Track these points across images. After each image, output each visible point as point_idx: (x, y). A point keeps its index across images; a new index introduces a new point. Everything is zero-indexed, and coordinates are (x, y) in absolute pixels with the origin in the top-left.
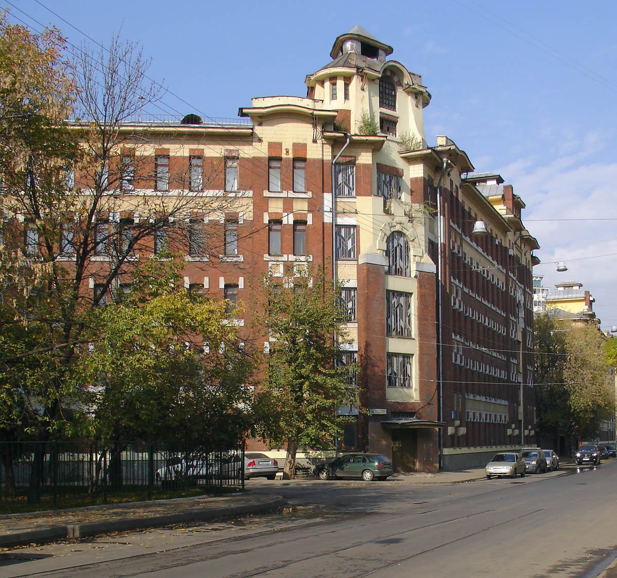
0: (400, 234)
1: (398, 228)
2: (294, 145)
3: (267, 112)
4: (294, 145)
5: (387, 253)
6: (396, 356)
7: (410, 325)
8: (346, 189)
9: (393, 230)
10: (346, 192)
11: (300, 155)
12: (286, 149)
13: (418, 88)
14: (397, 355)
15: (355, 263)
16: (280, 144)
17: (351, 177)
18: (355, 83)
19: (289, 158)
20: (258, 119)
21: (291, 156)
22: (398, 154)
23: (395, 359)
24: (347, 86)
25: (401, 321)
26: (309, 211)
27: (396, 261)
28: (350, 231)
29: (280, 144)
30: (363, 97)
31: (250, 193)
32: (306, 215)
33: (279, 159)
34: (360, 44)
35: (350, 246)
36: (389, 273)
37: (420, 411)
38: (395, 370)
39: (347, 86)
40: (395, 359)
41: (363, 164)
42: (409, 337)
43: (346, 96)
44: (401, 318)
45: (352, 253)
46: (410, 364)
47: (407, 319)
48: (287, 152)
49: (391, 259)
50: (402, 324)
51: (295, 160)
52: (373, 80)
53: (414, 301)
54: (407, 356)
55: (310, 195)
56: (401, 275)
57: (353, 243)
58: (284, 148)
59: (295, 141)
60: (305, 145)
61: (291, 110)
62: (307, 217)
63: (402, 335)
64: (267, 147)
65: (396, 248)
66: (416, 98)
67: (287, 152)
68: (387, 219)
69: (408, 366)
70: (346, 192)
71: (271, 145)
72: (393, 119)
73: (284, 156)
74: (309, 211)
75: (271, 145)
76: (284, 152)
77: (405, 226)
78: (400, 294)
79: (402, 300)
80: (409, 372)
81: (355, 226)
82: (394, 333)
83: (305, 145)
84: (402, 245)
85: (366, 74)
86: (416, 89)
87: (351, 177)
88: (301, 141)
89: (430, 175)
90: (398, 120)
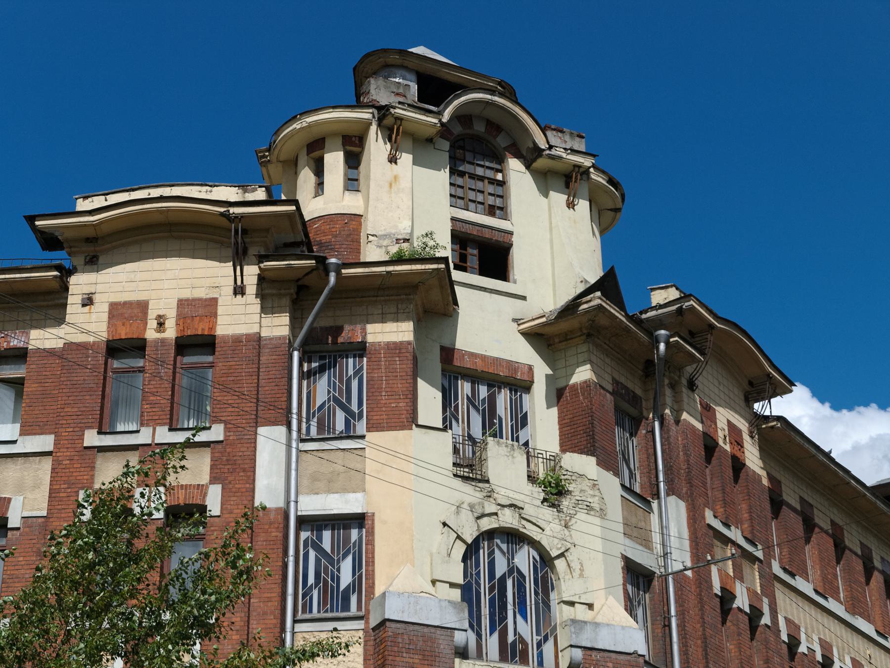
0: (515, 537)
1: (508, 519)
2: (182, 303)
3: (102, 222)
4: (182, 303)
5: (469, 592)
8: (340, 417)
9: (487, 524)
10: (340, 426)
11: (200, 328)
12: (159, 317)
13: (564, 155)
15: (360, 624)
16: (143, 307)
17: (355, 384)
19: (163, 341)
20: (90, 249)
21: (171, 333)
22: (515, 325)
24: (353, 160)
26: (213, 480)
27: (504, 618)
28: (347, 539)
29: (143, 307)
30: (396, 178)
31: (45, 442)
32: (202, 489)
33: (138, 347)
34: (414, 77)
35: (346, 578)
39: (353, 160)
41: (388, 344)
43: (352, 183)
45: (354, 599)
48: (161, 325)
49: (485, 611)
51: (184, 345)
52: (430, 140)
55: (217, 433)
57: (356, 567)
58: (152, 314)
59: (187, 294)
60: (212, 304)
61: (168, 210)
62: (205, 495)
64: (105, 317)
65: (503, 580)
66: (567, 186)
67: (161, 325)
68: (469, 493)
70: (340, 426)
71: (117, 311)
72: (497, 237)
73: (151, 334)
74: (213, 480)
75: (117, 311)
76: (152, 324)
77: (530, 511)
81: (359, 520)
83: (212, 304)
84: (525, 571)
85: (399, 119)
86: (561, 158)
87: (355, 384)
88: (201, 293)
89: (623, 380)
90: (515, 239)
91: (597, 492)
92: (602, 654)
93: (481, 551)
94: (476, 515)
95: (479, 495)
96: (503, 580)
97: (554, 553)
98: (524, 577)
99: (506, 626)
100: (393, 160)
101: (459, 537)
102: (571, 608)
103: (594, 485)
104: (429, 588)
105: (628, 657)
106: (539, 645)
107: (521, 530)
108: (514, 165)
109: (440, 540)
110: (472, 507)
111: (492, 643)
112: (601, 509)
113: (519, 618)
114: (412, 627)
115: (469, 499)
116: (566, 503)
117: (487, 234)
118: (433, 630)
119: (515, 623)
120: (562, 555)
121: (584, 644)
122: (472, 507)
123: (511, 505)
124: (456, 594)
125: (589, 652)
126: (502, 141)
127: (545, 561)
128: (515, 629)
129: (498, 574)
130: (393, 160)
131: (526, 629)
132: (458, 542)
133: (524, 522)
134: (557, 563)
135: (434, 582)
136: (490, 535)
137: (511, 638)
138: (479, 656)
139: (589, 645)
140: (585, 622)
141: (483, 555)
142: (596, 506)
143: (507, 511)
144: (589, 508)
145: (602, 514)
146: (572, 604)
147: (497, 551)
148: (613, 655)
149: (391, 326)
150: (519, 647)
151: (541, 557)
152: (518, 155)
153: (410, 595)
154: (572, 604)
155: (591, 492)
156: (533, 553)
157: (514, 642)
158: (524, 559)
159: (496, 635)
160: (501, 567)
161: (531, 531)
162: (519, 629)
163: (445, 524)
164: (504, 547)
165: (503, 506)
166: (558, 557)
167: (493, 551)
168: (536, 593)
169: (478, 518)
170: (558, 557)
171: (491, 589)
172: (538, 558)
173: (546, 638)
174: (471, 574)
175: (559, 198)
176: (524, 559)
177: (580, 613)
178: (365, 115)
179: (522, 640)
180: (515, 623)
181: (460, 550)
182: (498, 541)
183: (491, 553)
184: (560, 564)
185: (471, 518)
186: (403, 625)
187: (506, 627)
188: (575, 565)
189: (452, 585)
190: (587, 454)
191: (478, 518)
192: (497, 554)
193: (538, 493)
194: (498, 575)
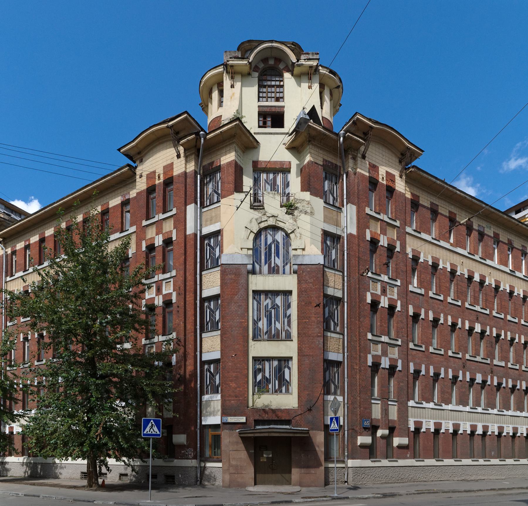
0: (275, 228)
1: (271, 222)
5: (256, 250)
6: (267, 360)
7: (290, 327)
9: (263, 225)
14: (269, 359)
18: (227, 82)
23: (267, 364)
25: (277, 322)
27: (270, 258)
36: (253, 272)
37: (297, 418)
38: (267, 375)
40: (267, 364)
42: (288, 337)
44: (277, 318)
46: (289, 368)
47: (286, 320)
50: (279, 326)
53: (294, 299)
54: (285, 361)
56: (278, 272)
63: (278, 337)
65: (270, 245)
68: (256, 214)
69: (287, 371)
72: (278, 110)
78: (276, 293)
79: (279, 300)
80: (287, 377)
82: (266, 337)
91: (310, 206)
92: (305, 266)
93: (262, 236)
94: (258, 222)
95: (260, 215)
96: (270, 245)
97: (289, 232)
98: (279, 243)
99: (271, 262)
100: (232, 86)
101: (251, 231)
102: (296, 251)
103: (309, 203)
104: (240, 251)
105: (316, 266)
106: (284, 267)
107: (277, 225)
108: (287, 75)
109: (244, 233)
110: (257, 220)
111: (265, 268)
112: (311, 212)
113: (276, 258)
114: (231, 266)
115: (256, 217)
116: (296, 213)
117: (273, 110)
118: (239, 266)
119: (275, 260)
120: (293, 232)
121: (298, 263)
122: (257, 220)
123: (273, 216)
124: (250, 252)
125: (300, 266)
126: (281, 66)
127: (288, 235)
128: (275, 262)
129: (269, 243)
130: (232, 86)
131: (279, 262)
132: (252, 233)
133: (278, 222)
134: (291, 235)
135: (241, 249)
136: (266, 228)
137: (273, 265)
138: (260, 273)
139: (300, 263)
140: (299, 255)
141: (263, 237)
142: (309, 211)
143: (271, 219)
144: (306, 213)
145: (312, 213)
146: (296, 249)
147: (268, 235)
148: (310, 266)
149: (228, 156)
150: (276, 268)
151: (286, 234)
152: (288, 71)
153: (230, 254)
154: (296, 249)
155: (307, 206)
156: (283, 233)
157: (274, 267)
158: (279, 236)
159: (267, 265)
160: (270, 240)
161: (281, 225)
162: (276, 262)
163: (246, 227)
164: (271, 233)
165: (269, 217)
166: (291, 233)
167: (267, 235)
168: (284, 248)
169: (259, 223)
170: (291, 233)
171: (265, 249)
172: (285, 235)
173: (287, 264)
174: (258, 245)
175: (305, 85)
176: (279, 236)
177: (299, 252)
178: (220, 69)
179: (278, 266)
180: (275, 260)
181: (252, 236)
182: (269, 231)
183: (266, 236)
184: (292, 236)
185: (256, 224)
186: (228, 265)
187: (271, 262)
188: (298, 235)
189: (248, 249)
190: (306, 191)
191: (259, 223)
192: (269, 236)
193: (284, 210)
194: (269, 243)
